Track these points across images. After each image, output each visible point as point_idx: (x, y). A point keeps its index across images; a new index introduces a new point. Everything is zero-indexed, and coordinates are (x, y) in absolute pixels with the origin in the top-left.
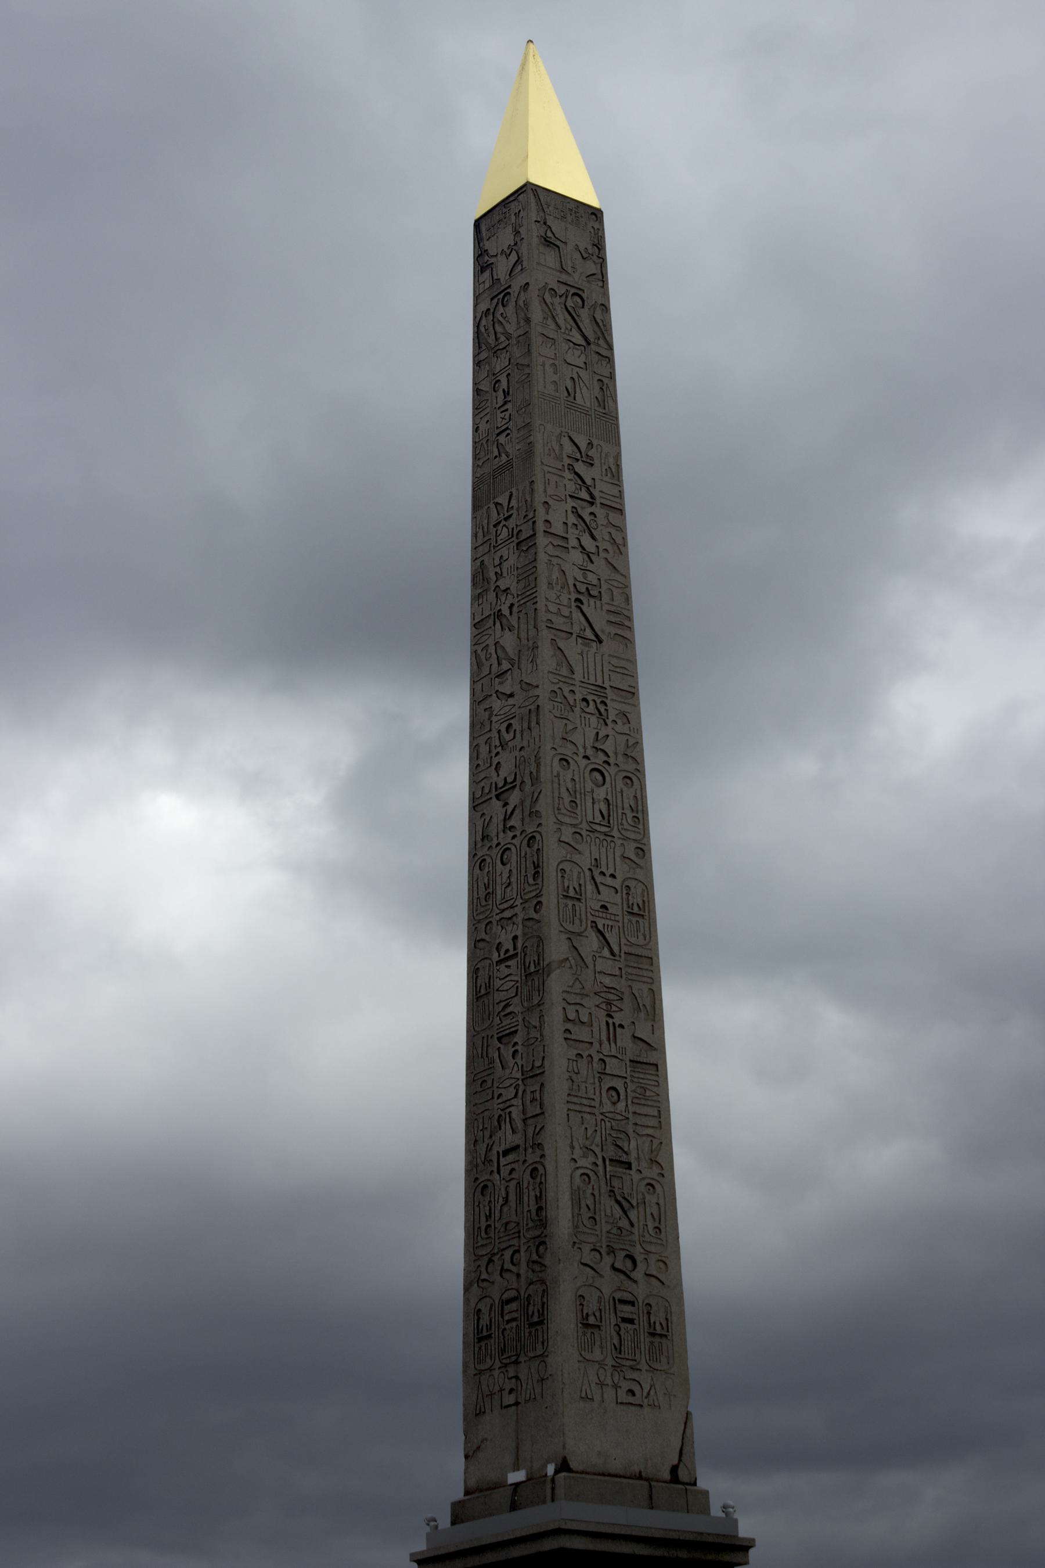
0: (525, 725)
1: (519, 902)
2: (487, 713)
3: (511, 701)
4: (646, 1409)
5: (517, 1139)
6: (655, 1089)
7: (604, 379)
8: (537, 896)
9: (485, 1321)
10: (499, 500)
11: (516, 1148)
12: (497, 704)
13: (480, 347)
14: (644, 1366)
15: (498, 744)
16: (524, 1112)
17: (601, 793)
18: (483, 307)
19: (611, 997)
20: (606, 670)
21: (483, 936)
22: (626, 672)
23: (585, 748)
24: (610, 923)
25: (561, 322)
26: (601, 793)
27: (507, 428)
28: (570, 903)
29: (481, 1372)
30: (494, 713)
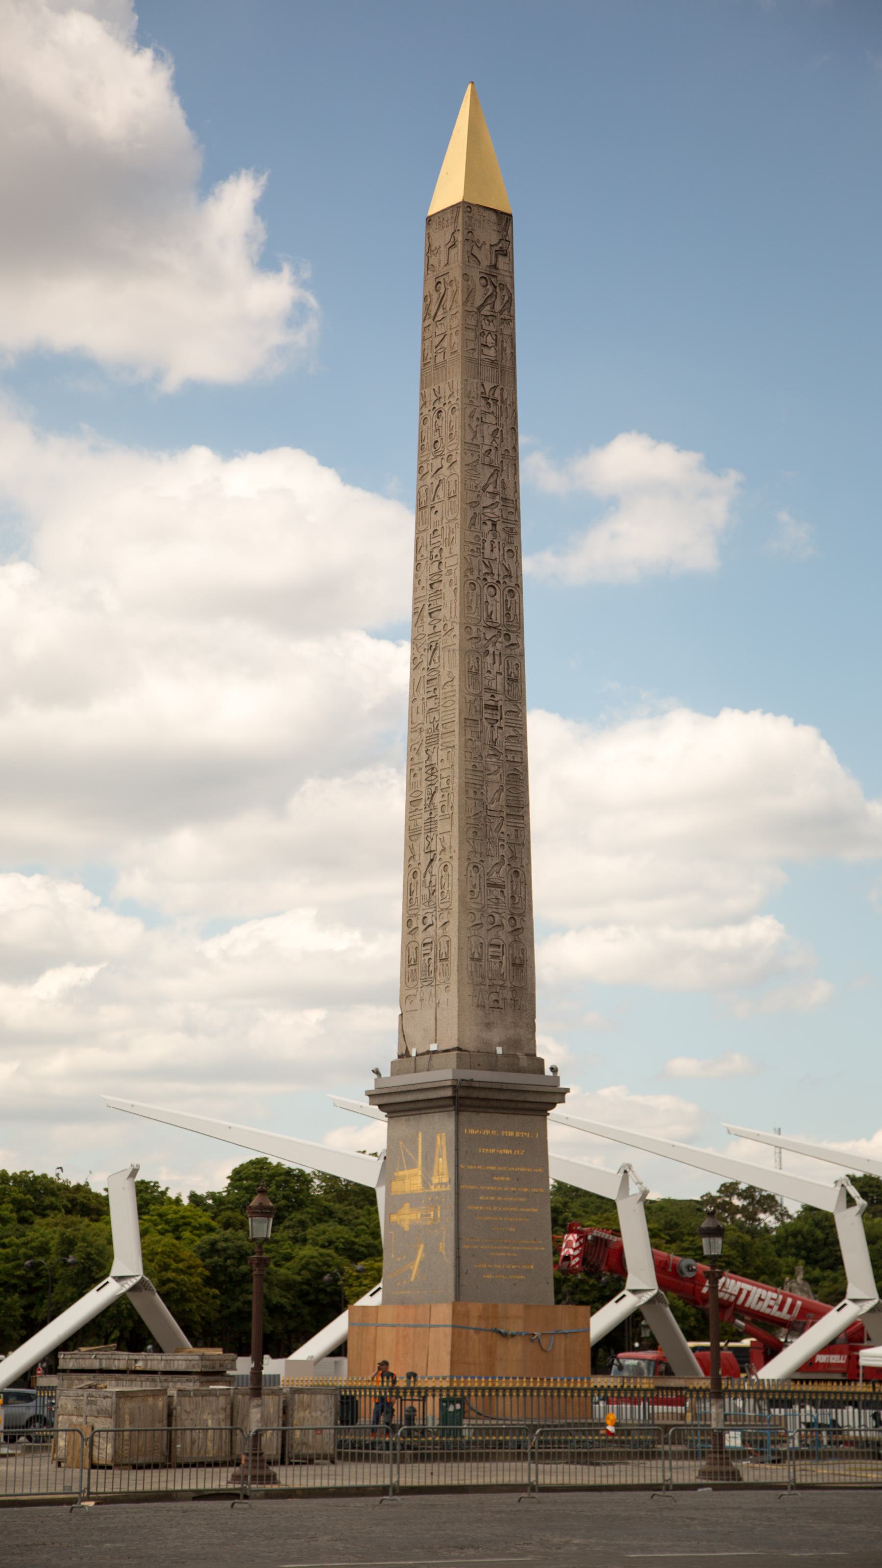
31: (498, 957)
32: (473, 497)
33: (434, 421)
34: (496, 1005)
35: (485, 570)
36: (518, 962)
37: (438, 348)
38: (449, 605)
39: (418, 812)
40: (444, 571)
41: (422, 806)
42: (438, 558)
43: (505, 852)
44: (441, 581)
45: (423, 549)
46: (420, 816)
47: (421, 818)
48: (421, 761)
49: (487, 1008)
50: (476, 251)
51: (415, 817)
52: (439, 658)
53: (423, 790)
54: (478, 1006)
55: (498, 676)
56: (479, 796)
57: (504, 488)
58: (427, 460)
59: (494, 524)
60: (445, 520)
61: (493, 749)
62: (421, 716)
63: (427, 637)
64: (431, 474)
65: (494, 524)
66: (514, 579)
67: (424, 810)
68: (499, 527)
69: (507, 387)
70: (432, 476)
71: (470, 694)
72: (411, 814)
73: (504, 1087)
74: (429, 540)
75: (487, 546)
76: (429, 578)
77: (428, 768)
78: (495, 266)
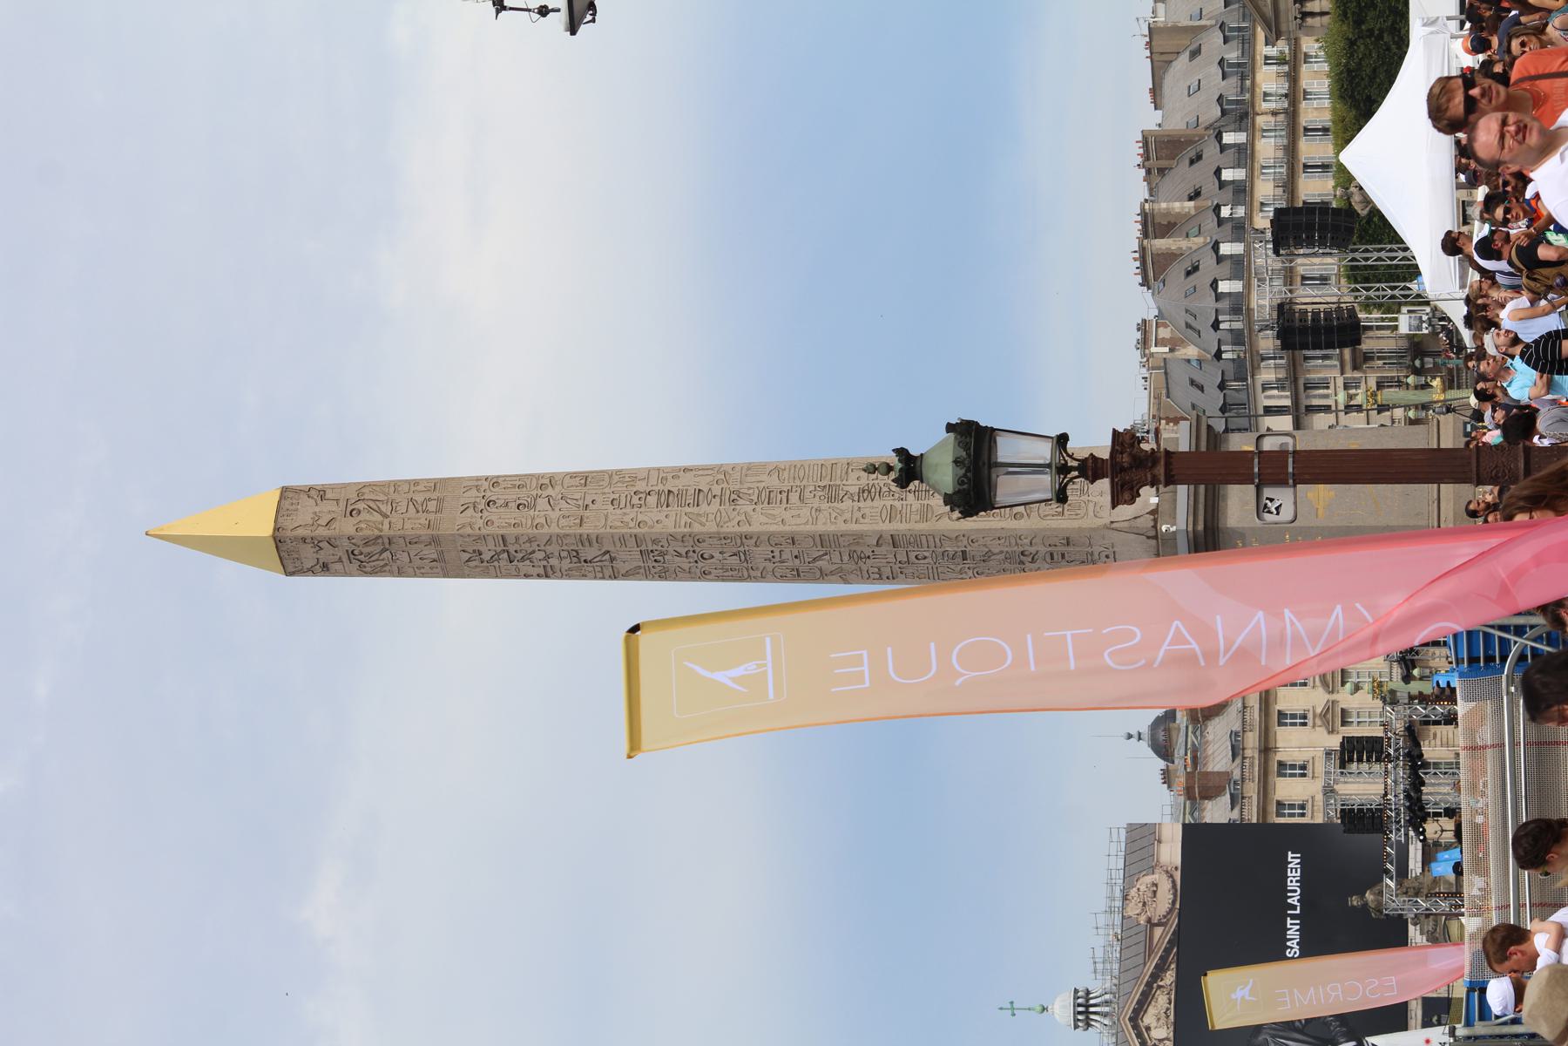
4: (1115, 549)
6: (908, 537)
7: (408, 541)
14: (1089, 550)
17: (717, 555)
19: (855, 556)
20: (628, 549)
22: (622, 539)
23: (690, 562)
24: (805, 555)
25: (382, 563)
26: (717, 555)
28: (802, 574)
33: (494, 510)
37: (420, 509)
38: (697, 479)
39: (904, 511)
40: (660, 487)
41: (898, 504)
42: (643, 496)
44: (669, 491)
45: (627, 519)
46: (909, 507)
47: (911, 505)
48: (850, 509)
51: (908, 515)
52: (749, 488)
53: (883, 503)
58: (533, 519)
60: (606, 490)
62: (805, 512)
63: (723, 507)
64: (550, 513)
67: (904, 502)
70: (553, 510)
72: (904, 520)
74: (619, 511)
76: (659, 508)
77: (861, 498)
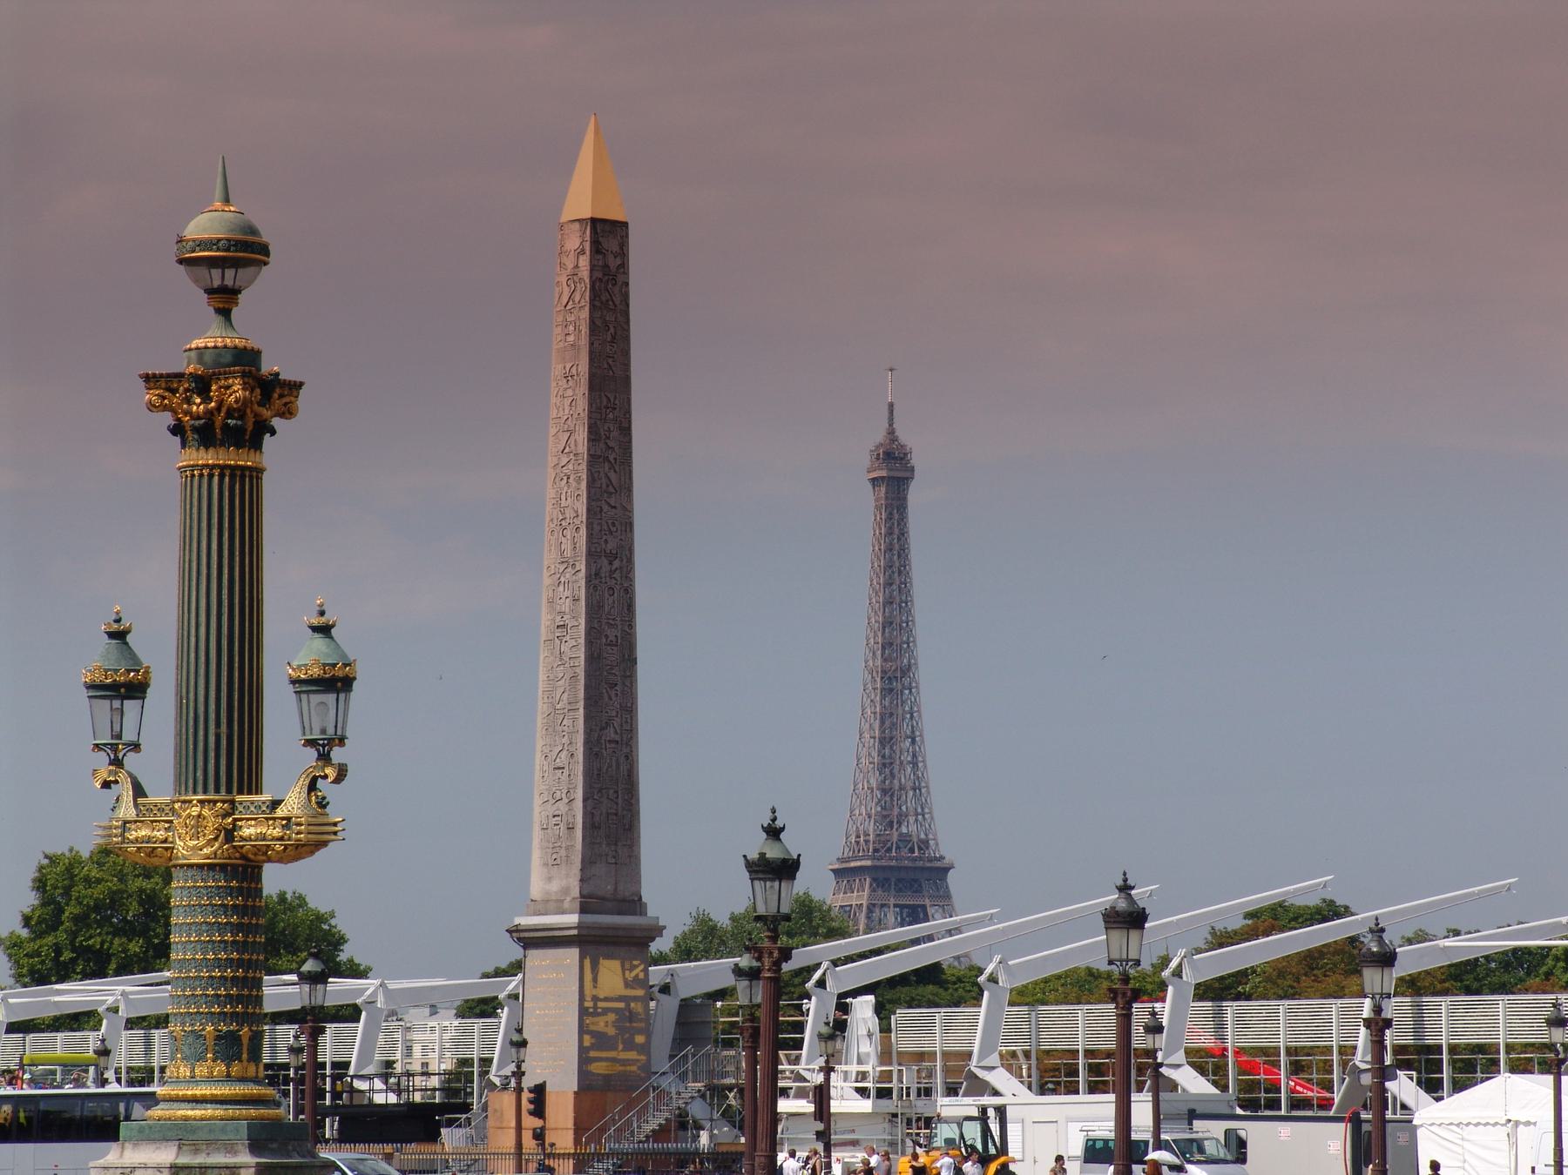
0: (623, 529)
1: (618, 619)
2: (599, 509)
3: (614, 510)
5: (617, 738)
8: (629, 621)
9: (597, 819)
10: (609, 395)
11: (617, 742)
12: (605, 508)
13: (595, 297)
15: (606, 528)
16: (622, 726)
18: (599, 274)
21: (596, 626)
27: (613, 357)
29: (594, 843)
30: (605, 511)
31: (558, 825)
32: (555, 460)
34: (555, 863)
35: (561, 518)
36: (570, 826)
43: (566, 740)
49: (550, 864)
50: (565, 260)
54: (544, 864)
55: (568, 600)
56: (551, 700)
57: (576, 446)
59: (568, 478)
61: (561, 659)
65: (568, 478)
66: (580, 517)
68: (571, 480)
69: (581, 362)
71: (549, 620)
73: (537, 928)
75: (563, 497)
78: (577, 266)
